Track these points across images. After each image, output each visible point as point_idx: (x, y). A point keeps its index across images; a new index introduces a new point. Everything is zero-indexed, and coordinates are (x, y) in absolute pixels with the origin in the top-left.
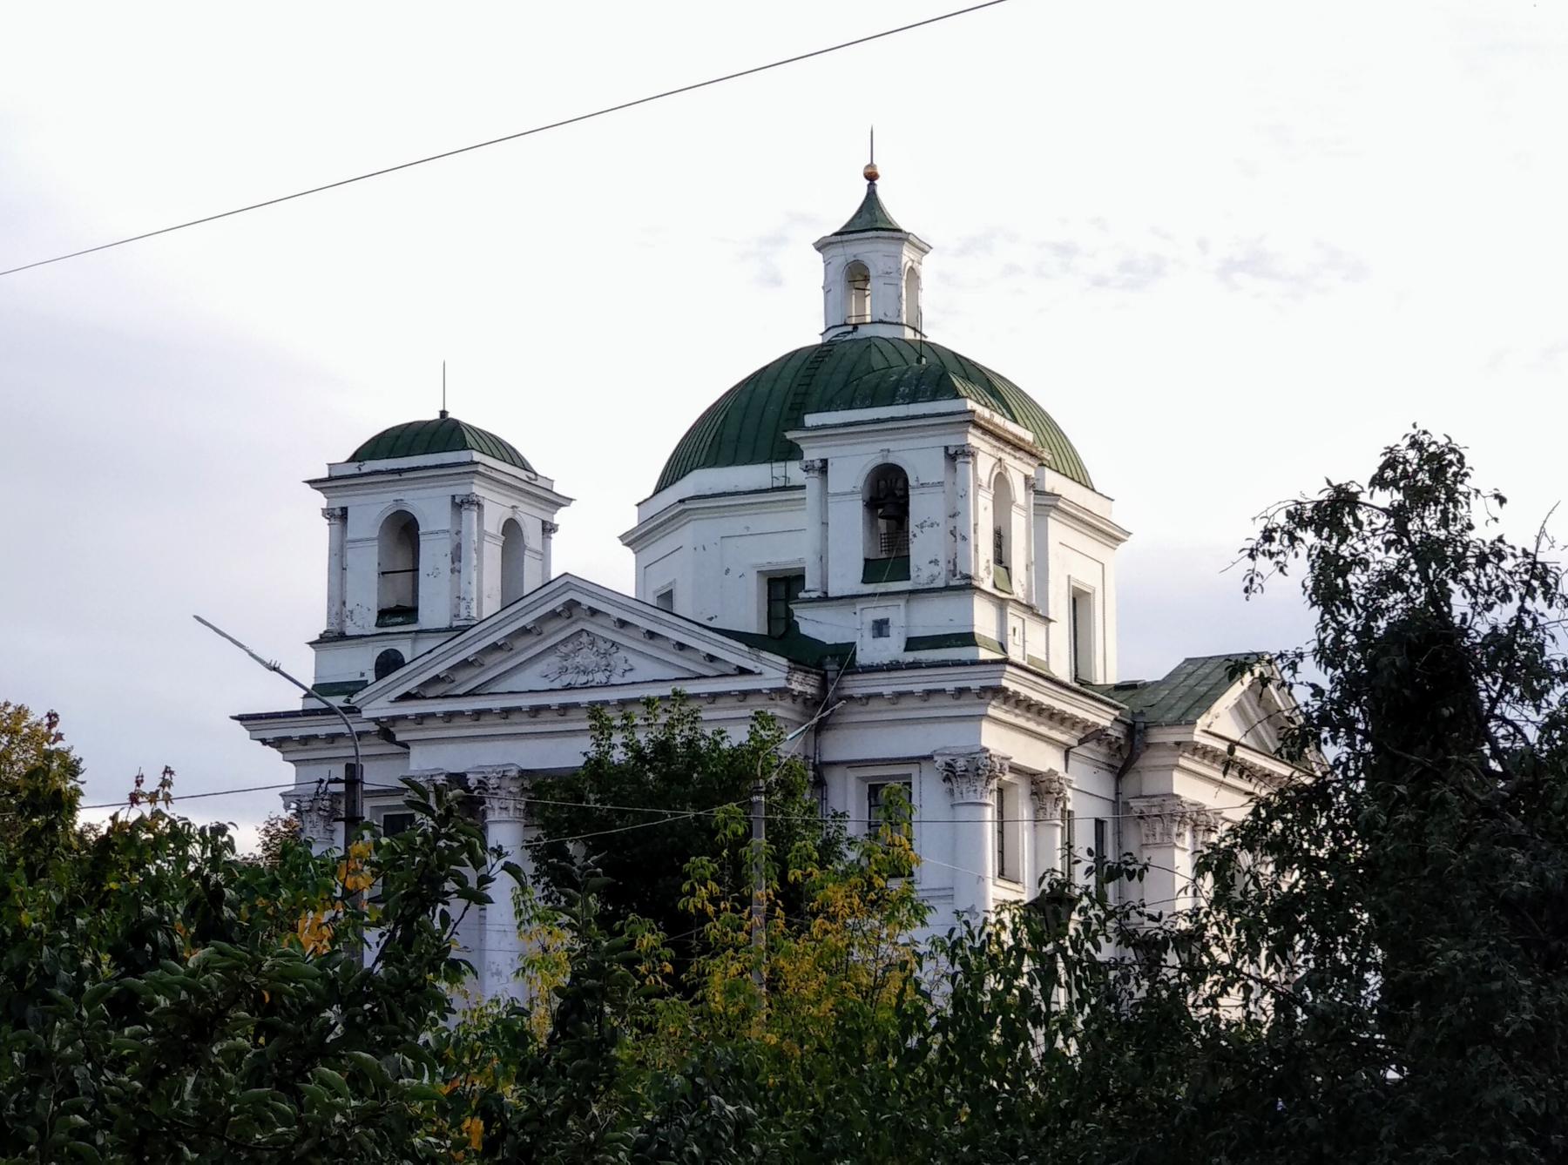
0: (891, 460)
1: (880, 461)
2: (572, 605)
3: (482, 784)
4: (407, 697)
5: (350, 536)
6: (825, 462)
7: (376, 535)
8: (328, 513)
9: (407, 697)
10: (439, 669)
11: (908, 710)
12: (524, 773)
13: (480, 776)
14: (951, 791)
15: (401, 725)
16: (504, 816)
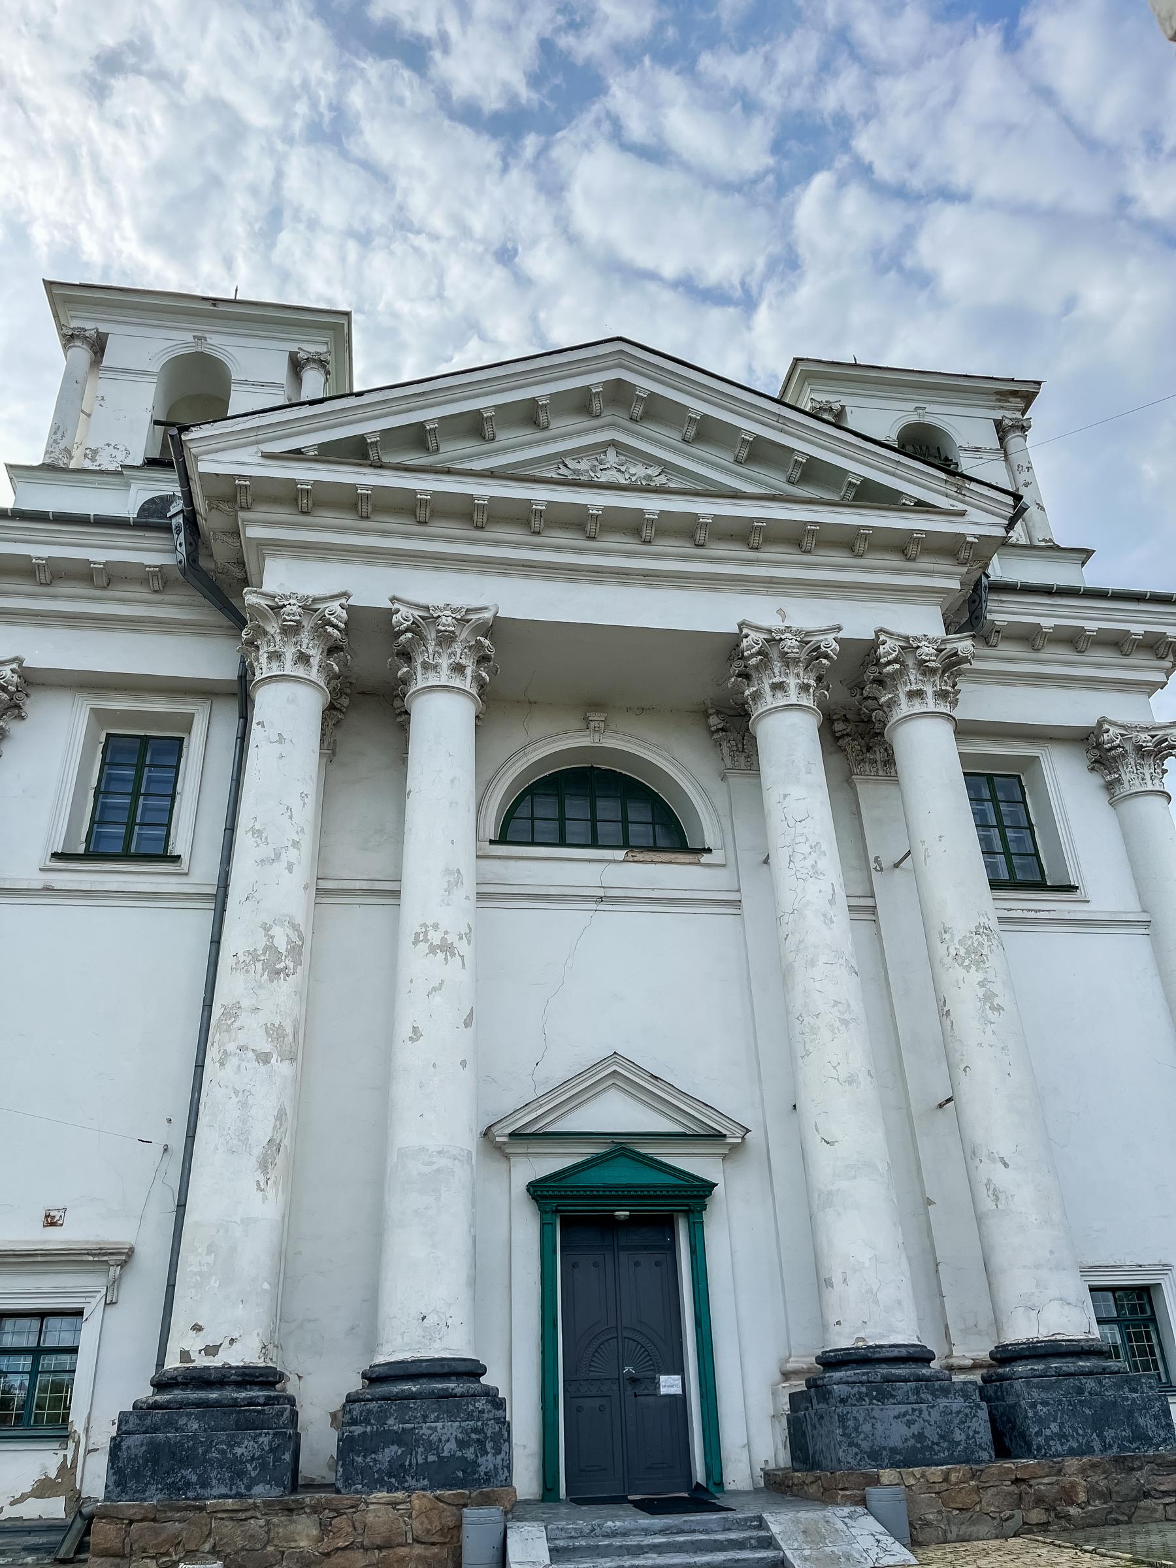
0: (929, 420)
1: (914, 418)
2: (619, 393)
3: (414, 628)
4: (297, 455)
5: (106, 361)
6: (843, 407)
7: (156, 368)
8: (69, 339)
9: (297, 455)
10: (369, 428)
11: (1056, 660)
12: (496, 628)
13: (416, 613)
14: (1110, 787)
15: (262, 512)
16: (457, 682)
